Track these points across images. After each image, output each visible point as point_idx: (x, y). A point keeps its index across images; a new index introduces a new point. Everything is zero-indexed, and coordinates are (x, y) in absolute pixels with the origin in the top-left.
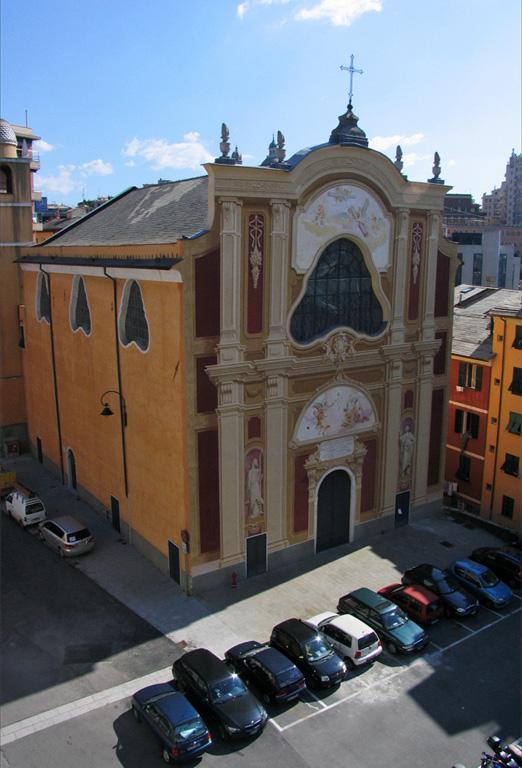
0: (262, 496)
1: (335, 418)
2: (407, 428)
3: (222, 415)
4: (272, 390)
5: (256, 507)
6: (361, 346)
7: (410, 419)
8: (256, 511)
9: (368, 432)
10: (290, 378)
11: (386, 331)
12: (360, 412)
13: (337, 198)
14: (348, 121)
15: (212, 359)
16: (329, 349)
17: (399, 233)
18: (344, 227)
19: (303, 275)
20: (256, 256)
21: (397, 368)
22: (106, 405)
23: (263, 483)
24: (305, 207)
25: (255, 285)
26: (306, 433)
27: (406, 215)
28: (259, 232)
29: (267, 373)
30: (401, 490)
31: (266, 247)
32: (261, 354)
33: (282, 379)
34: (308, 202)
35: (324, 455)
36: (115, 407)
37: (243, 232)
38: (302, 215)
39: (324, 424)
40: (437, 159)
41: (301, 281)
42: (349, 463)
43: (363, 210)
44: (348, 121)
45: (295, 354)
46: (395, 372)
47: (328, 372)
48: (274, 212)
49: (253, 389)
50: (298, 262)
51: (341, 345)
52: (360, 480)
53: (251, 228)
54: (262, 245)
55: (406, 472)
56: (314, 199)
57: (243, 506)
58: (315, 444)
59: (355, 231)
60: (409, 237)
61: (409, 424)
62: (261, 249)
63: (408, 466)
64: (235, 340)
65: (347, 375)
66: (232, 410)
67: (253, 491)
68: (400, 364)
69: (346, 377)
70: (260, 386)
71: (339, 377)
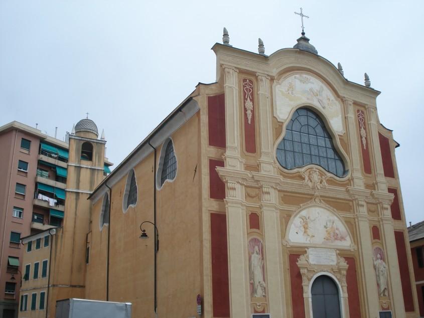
0: (264, 280)
1: (319, 234)
2: (379, 256)
3: (229, 204)
4: (266, 197)
5: (259, 286)
8: (260, 292)
11: (348, 176)
12: (337, 232)
13: (301, 81)
14: (304, 39)
15: (221, 164)
16: (307, 178)
17: (348, 113)
18: (308, 99)
19: (282, 123)
21: (362, 206)
22: (144, 231)
23: (263, 268)
24: (280, 82)
26: (296, 236)
27: (351, 103)
29: (262, 183)
30: (383, 309)
31: (256, 100)
32: (257, 168)
34: (281, 80)
36: (150, 231)
37: (240, 88)
38: (279, 86)
39: (310, 232)
41: (281, 126)
42: (334, 272)
45: (281, 174)
46: (361, 209)
47: (308, 194)
49: (253, 192)
50: (278, 114)
51: (316, 177)
52: (345, 289)
53: (244, 86)
54: (253, 98)
55: (384, 293)
56: (286, 78)
57: (249, 284)
61: (381, 254)
62: (252, 100)
63: (385, 289)
65: (324, 200)
66: (236, 203)
70: (257, 191)
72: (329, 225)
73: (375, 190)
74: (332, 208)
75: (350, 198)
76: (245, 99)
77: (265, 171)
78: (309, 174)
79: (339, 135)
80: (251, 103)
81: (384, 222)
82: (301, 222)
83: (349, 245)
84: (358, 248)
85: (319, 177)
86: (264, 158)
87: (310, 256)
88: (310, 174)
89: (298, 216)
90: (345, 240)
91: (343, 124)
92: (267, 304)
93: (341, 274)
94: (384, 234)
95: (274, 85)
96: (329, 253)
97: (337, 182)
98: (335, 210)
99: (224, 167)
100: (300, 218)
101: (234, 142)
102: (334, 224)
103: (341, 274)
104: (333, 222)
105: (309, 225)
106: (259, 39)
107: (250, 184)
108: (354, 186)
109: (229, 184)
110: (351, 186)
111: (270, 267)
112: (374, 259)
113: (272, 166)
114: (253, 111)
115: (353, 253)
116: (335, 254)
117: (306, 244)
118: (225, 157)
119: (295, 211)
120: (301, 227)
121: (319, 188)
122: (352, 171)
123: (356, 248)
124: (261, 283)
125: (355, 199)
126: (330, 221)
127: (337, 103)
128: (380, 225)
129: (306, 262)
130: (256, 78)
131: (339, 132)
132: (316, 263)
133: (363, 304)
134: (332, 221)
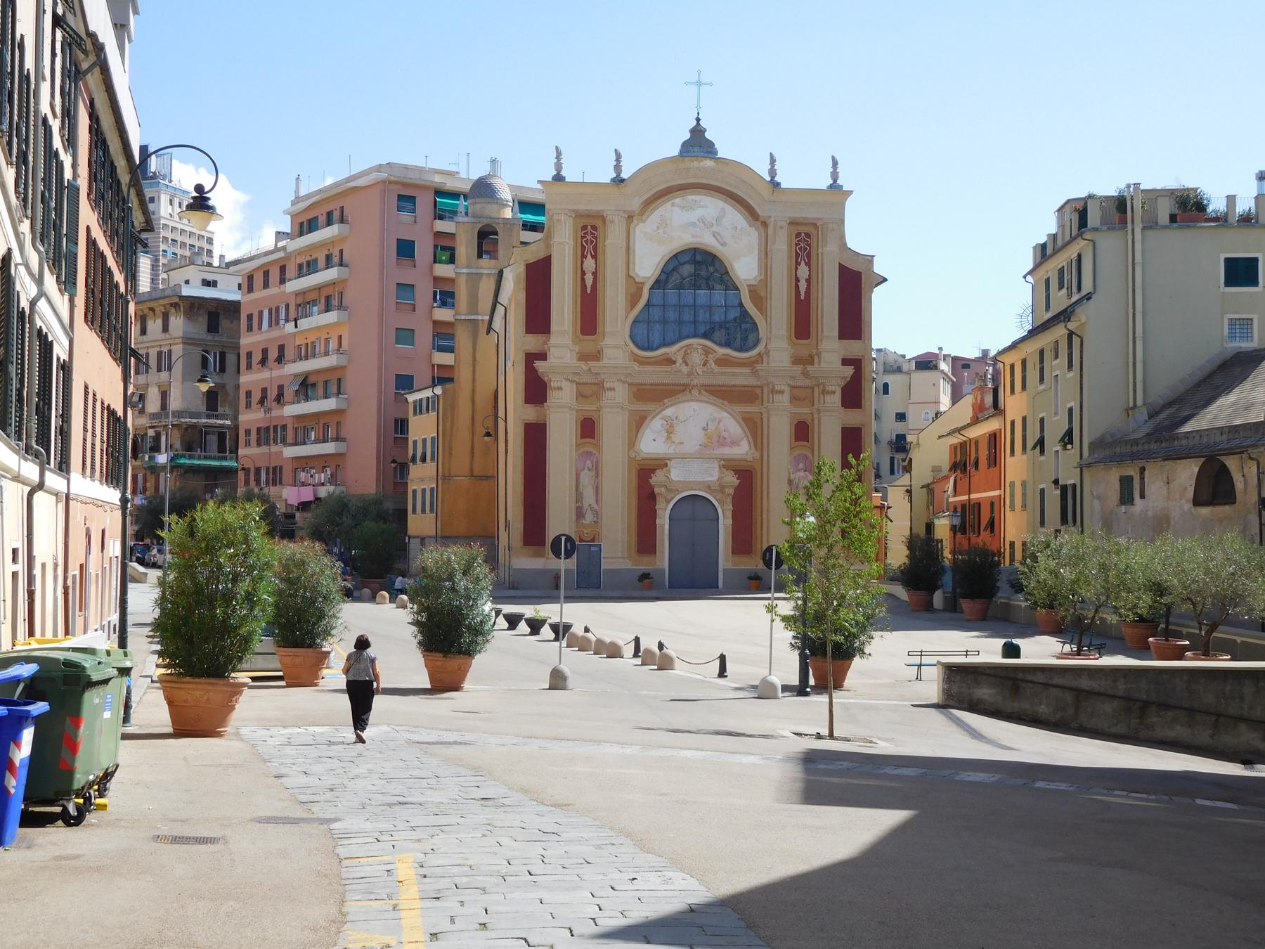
2: (801, 466)
3: (551, 410)
4: (609, 394)
6: (722, 362)
7: (806, 457)
8: (589, 518)
10: (630, 384)
11: (760, 348)
12: (725, 434)
13: (682, 208)
14: (698, 132)
15: (543, 356)
16: (680, 361)
18: (693, 236)
19: (643, 283)
20: (589, 264)
21: (781, 392)
24: (644, 218)
25: (589, 290)
26: (651, 443)
28: (592, 242)
29: (603, 376)
32: (596, 356)
33: (620, 384)
34: (647, 213)
35: (676, 473)
39: (676, 439)
40: (835, 163)
44: (698, 132)
46: (777, 397)
48: (607, 222)
50: (637, 270)
51: (696, 358)
52: (729, 514)
54: (596, 253)
56: (654, 209)
59: (707, 241)
60: (790, 246)
62: (595, 257)
64: (568, 340)
65: (706, 391)
67: (585, 493)
68: (787, 389)
69: (704, 392)
71: (695, 392)
72: (712, 427)
73: (812, 364)
74: (721, 401)
77: (610, 359)
78: (685, 354)
79: (747, 285)
80: (593, 261)
81: (822, 414)
82: (662, 425)
84: (762, 456)
85: (703, 356)
86: (608, 341)
87: (672, 470)
88: (686, 354)
89: (659, 416)
90: (739, 445)
91: (760, 266)
92: (598, 532)
93: (723, 492)
94: (819, 433)
95: (633, 225)
96: (707, 465)
97: (733, 359)
98: (726, 402)
99: (546, 360)
100: (662, 419)
101: (563, 324)
103: (723, 492)
104: (719, 422)
106: (616, 150)
107: (584, 379)
109: (552, 383)
110: (762, 363)
111: (606, 486)
112: (791, 471)
113: (621, 351)
114: (595, 274)
115: (750, 464)
116: (716, 465)
117: (669, 454)
118: (549, 347)
119: (655, 411)
120: (661, 431)
121: (700, 373)
122: (769, 339)
123: (757, 456)
124: (592, 506)
125: (768, 384)
126: (714, 420)
128: (813, 420)
129: (665, 479)
130: (604, 220)
131: (749, 280)
132: (682, 480)
133: (759, 534)
134: (718, 420)
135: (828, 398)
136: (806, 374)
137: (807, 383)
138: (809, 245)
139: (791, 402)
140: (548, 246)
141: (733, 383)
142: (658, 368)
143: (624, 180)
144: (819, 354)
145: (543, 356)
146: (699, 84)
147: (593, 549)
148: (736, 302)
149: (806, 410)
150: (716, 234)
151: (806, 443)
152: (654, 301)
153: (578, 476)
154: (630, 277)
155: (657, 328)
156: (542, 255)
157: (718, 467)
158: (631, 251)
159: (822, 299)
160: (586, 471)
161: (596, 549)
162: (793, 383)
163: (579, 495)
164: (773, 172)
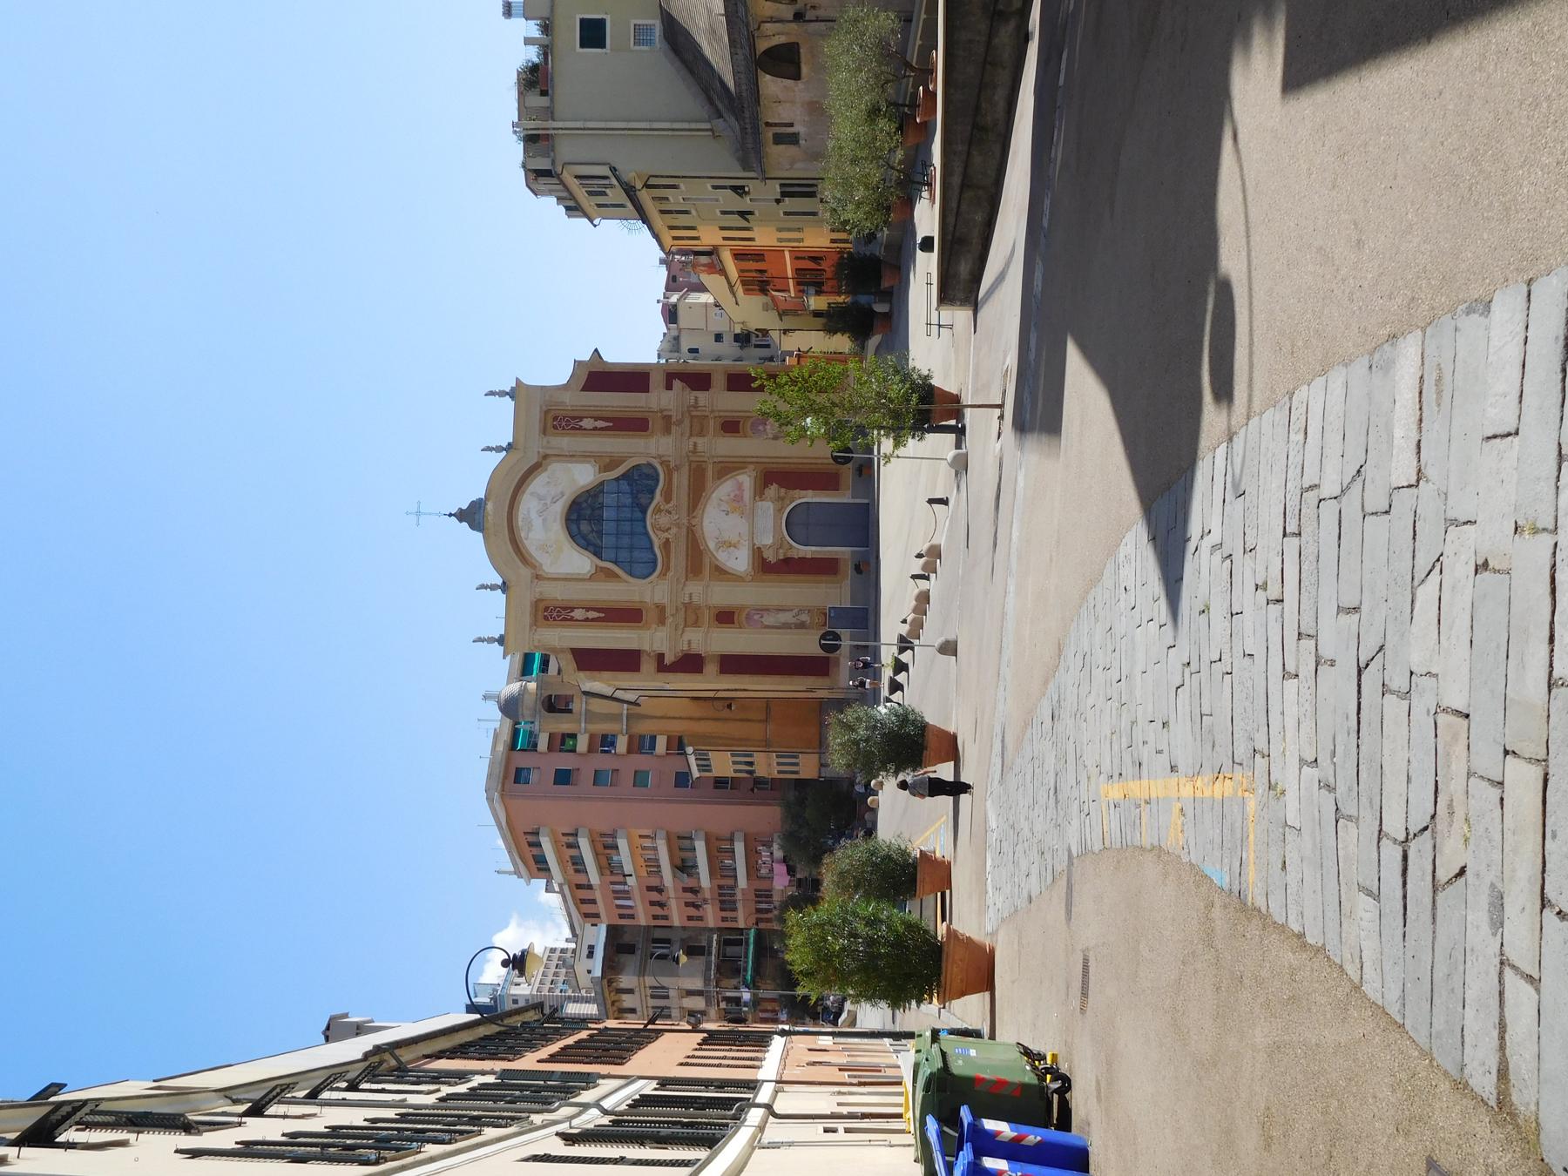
0: (792, 610)
2: (761, 428)
4: (695, 599)
6: (668, 497)
7: (752, 423)
8: (805, 617)
9: (755, 482)
12: (732, 497)
13: (529, 530)
14: (461, 516)
15: (661, 657)
18: (555, 521)
19: (596, 566)
20: (578, 614)
21: (695, 444)
23: (780, 610)
24: (537, 565)
26: (739, 561)
31: (571, 605)
32: (661, 609)
33: (686, 588)
34: (533, 561)
35: (767, 540)
37: (557, 626)
38: (544, 568)
39: (734, 539)
40: (492, 393)
41: (602, 569)
43: (540, 498)
44: (461, 516)
46: (700, 448)
47: (688, 536)
50: (585, 571)
51: (664, 520)
52: (803, 492)
56: (530, 555)
57: (796, 631)
58: (753, 550)
59: (559, 508)
62: (572, 609)
64: (646, 634)
65: (693, 511)
67: (783, 620)
68: (693, 439)
69: (695, 514)
73: (670, 416)
74: (702, 499)
75: (687, 464)
76: (572, 619)
78: (661, 530)
81: (715, 408)
83: (748, 479)
85: (663, 514)
86: (647, 599)
89: (715, 553)
90: (742, 483)
94: (732, 411)
98: (704, 494)
100: (717, 551)
102: (723, 498)
104: (721, 500)
105: (726, 538)
108: (669, 456)
114: (588, 609)
120: (729, 552)
123: (752, 467)
125: (688, 456)
126: (719, 505)
127: (549, 468)
128: (720, 417)
132: (772, 534)
135: (701, 403)
136: (679, 423)
137: (687, 422)
138: (564, 417)
139: (704, 436)
140: (562, 651)
141: (686, 487)
142: (673, 555)
143: (503, 582)
144: (661, 411)
145: (661, 657)
146: (418, 513)
147: (832, 615)
148: (615, 483)
149: (712, 422)
150: (554, 500)
151: (741, 423)
152: (613, 556)
153: (767, 627)
154: (591, 578)
155: (636, 554)
156: (570, 656)
157: (760, 503)
158: (569, 577)
159: (613, 407)
160: (763, 620)
161: (832, 611)
162: (688, 435)
163: (786, 626)
164: (499, 449)
